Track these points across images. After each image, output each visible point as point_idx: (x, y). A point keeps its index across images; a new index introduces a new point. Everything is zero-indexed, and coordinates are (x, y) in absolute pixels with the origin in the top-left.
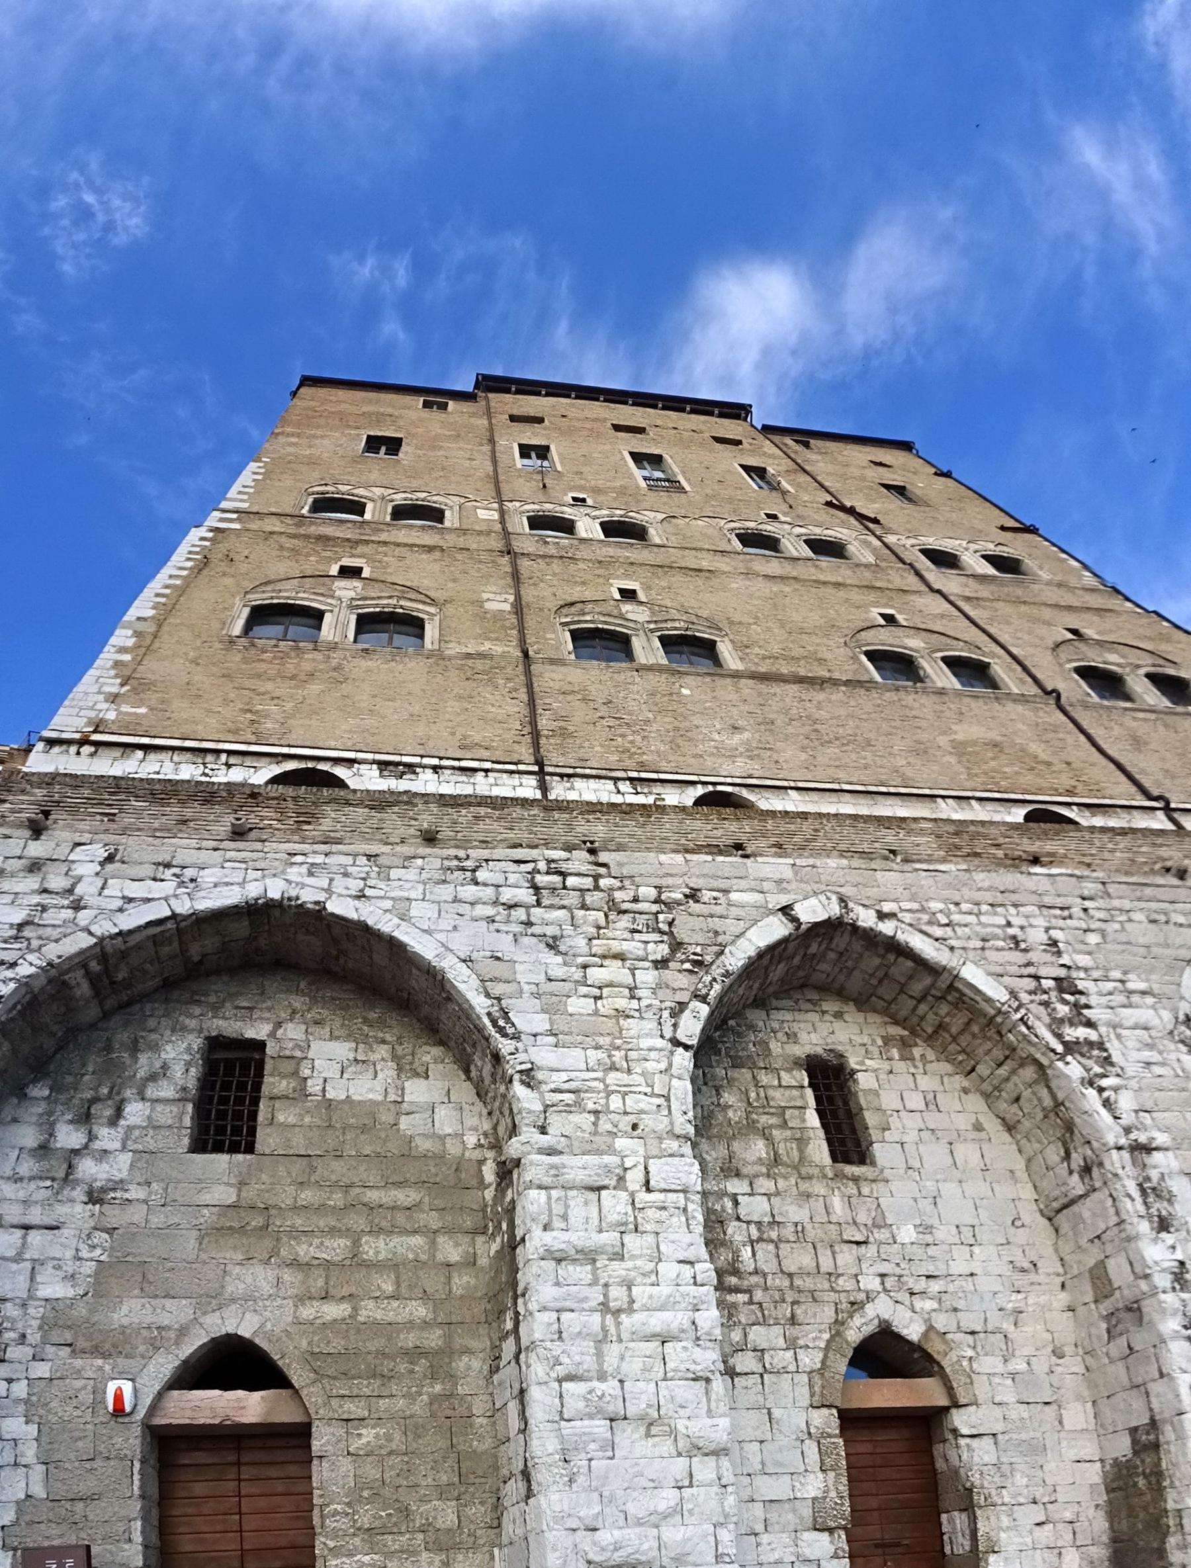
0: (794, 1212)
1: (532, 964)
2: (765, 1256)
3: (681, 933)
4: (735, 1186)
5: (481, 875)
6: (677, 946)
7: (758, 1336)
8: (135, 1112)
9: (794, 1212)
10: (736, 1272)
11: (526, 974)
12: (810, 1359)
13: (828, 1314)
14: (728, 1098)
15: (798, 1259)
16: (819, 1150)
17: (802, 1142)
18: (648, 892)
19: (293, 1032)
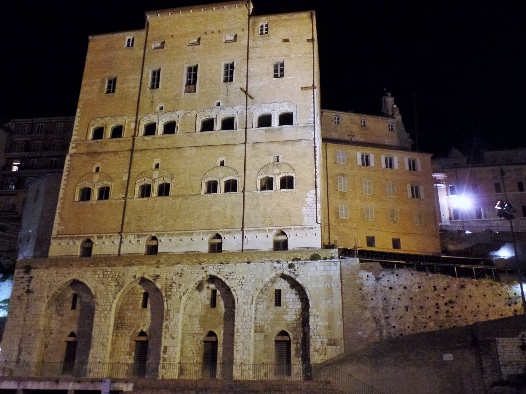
0: (134, 316)
1: (102, 287)
2: (129, 321)
3: (120, 281)
4: (127, 312)
5: (98, 273)
6: (119, 283)
7: (126, 331)
8: (65, 305)
9: (134, 316)
10: (124, 323)
11: (100, 289)
12: (130, 334)
13: (135, 329)
14: (130, 299)
15: (133, 321)
16: (140, 306)
17: (137, 306)
18: (117, 274)
19: (81, 293)
